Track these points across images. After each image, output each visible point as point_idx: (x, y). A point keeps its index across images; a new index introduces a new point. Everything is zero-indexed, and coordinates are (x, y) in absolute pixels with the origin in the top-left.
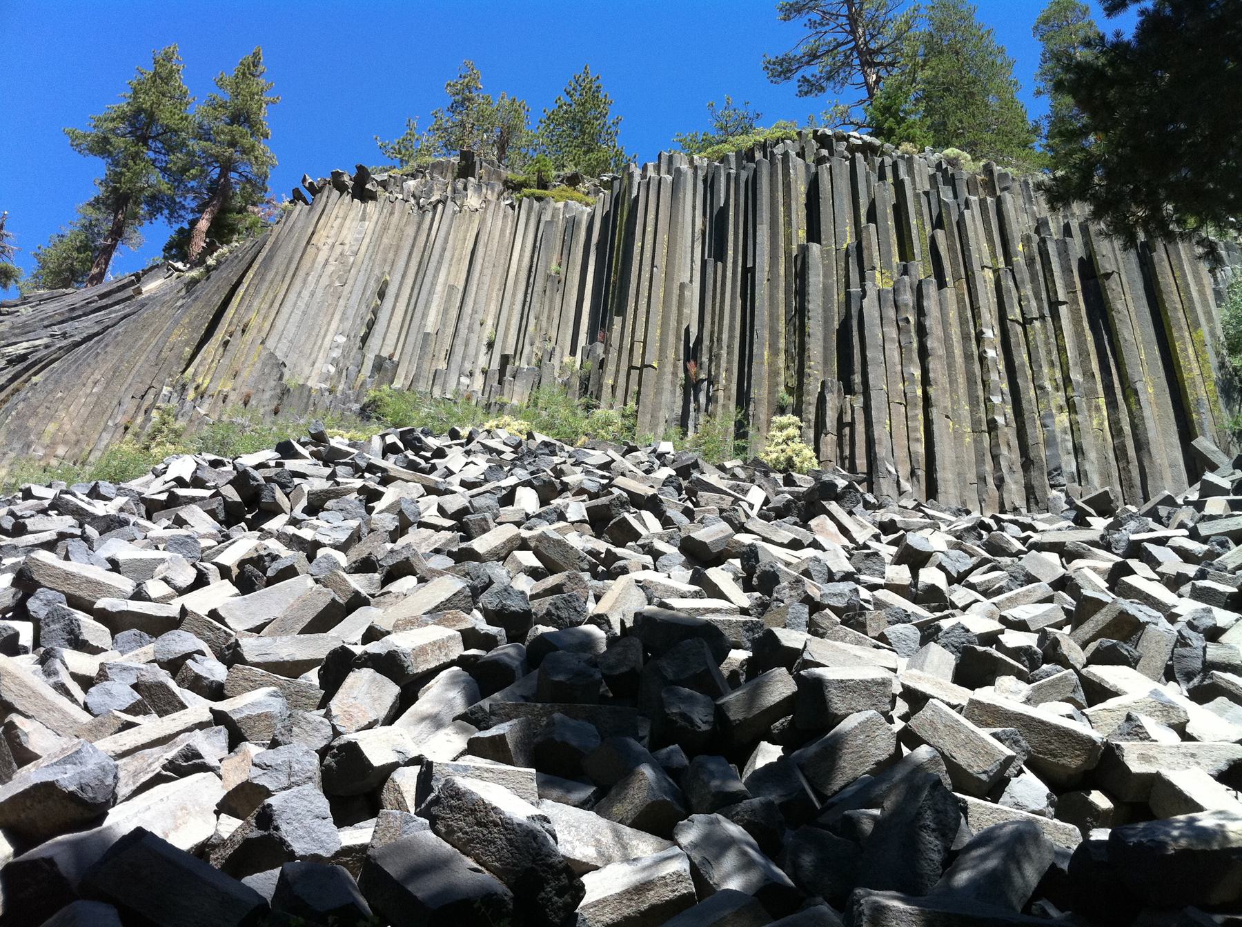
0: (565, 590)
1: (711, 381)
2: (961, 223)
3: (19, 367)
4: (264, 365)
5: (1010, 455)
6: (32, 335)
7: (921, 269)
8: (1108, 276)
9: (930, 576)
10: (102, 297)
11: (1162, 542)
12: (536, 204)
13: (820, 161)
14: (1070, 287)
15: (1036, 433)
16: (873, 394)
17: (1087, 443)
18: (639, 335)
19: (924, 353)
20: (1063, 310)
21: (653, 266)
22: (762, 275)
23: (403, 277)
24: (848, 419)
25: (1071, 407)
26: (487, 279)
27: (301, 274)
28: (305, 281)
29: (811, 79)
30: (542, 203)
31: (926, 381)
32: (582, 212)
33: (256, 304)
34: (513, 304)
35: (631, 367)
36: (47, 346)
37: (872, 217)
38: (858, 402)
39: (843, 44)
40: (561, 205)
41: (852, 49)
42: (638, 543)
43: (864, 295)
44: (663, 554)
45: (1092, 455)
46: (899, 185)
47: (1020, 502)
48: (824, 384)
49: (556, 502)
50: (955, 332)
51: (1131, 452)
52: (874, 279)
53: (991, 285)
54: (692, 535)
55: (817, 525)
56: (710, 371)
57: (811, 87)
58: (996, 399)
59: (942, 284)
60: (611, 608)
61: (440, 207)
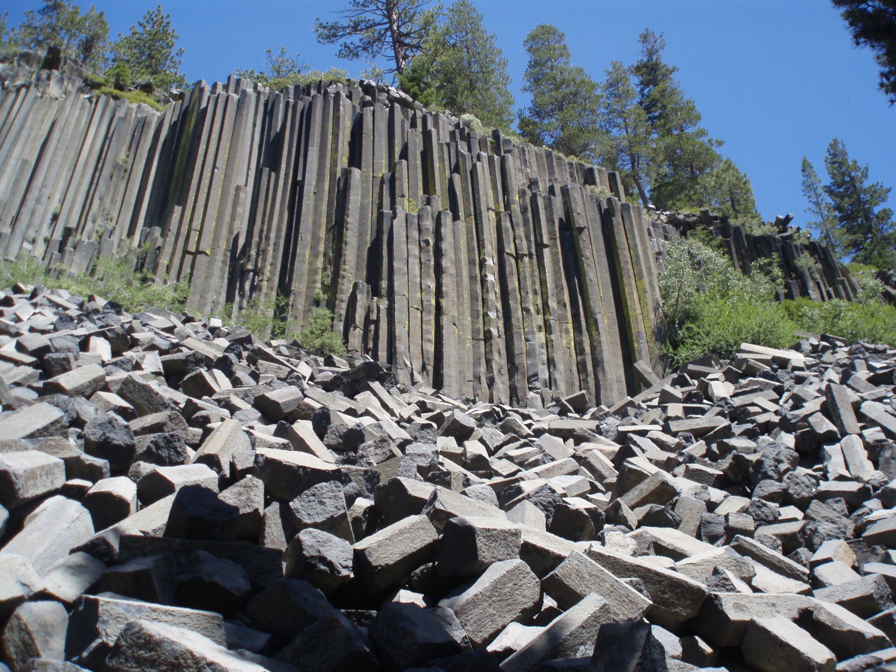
0: (165, 429)
1: (257, 271)
2: (474, 171)
5: (500, 361)
7: (440, 202)
8: (581, 230)
9: (473, 447)
11: (643, 433)
12: (112, 102)
13: (364, 104)
14: (551, 233)
15: (520, 346)
16: (397, 298)
17: (558, 357)
18: (196, 224)
19: (439, 271)
20: (546, 251)
21: (214, 167)
24: (374, 317)
29: (351, 46)
30: (118, 102)
31: (439, 293)
32: (153, 115)
34: (80, 184)
35: (186, 252)
37: (404, 155)
38: (384, 304)
39: (379, 24)
40: (134, 106)
41: (387, 30)
42: (214, 397)
43: (394, 216)
44: (239, 409)
45: (561, 367)
46: (427, 135)
47: (505, 398)
48: (356, 286)
49: (128, 354)
50: (464, 256)
51: (590, 368)
52: (403, 205)
53: (493, 224)
54: (267, 394)
55: (363, 400)
56: (256, 263)
57: (350, 52)
58: (492, 315)
59: (456, 217)
60: (222, 449)
61: (24, 90)
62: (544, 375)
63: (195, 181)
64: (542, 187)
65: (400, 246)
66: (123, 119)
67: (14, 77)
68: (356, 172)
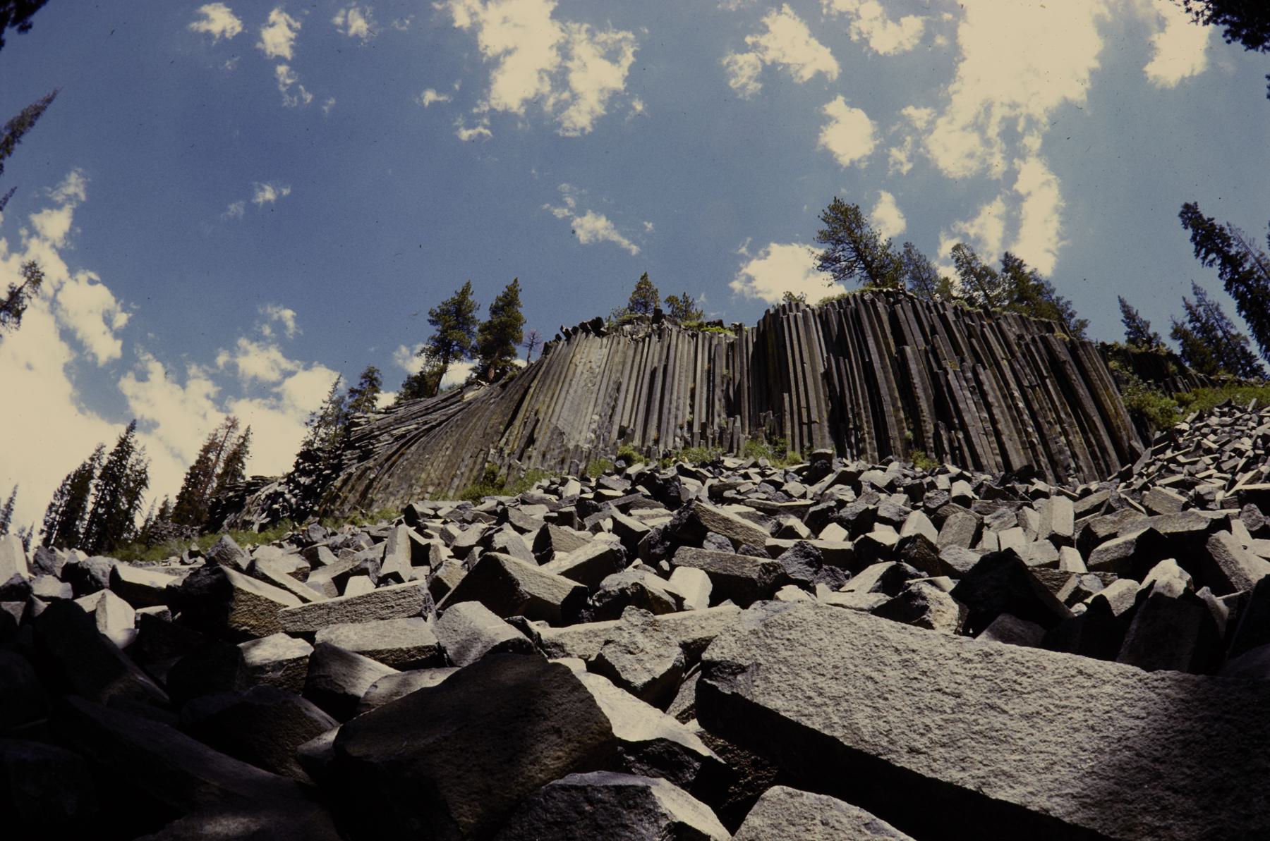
1: (858, 428)
2: (983, 333)
3: (403, 441)
4: (552, 433)
6: (407, 423)
7: (969, 362)
10: (443, 401)
14: (1046, 368)
15: (1054, 447)
16: (970, 428)
17: (1078, 451)
18: (803, 403)
19: (988, 407)
20: (1048, 381)
21: (802, 363)
22: (877, 365)
23: (630, 378)
24: (956, 444)
25: (1066, 434)
26: (683, 379)
27: (568, 380)
28: (570, 384)
33: (541, 398)
34: (701, 393)
35: (801, 424)
36: (416, 429)
37: (934, 331)
38: (961, 435)
43: (946, 373)
45: (1081, 457)
48: (936, 426)
56: (855, 422)
58: (1030, 430)
59: (985, 368)
61: (647, 339)
62: (1073, 465)
63: (792, 375)
64: (1028, 338)
65: (958, 394)
66: (719, 344)
67: (637, 333)
68: (908, 349)
